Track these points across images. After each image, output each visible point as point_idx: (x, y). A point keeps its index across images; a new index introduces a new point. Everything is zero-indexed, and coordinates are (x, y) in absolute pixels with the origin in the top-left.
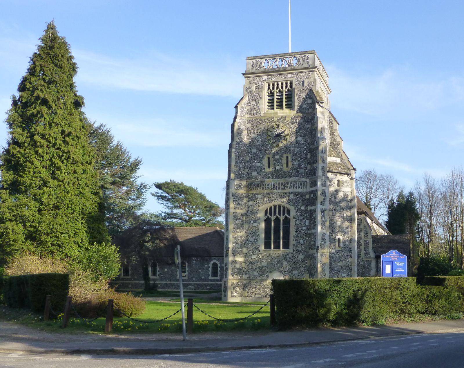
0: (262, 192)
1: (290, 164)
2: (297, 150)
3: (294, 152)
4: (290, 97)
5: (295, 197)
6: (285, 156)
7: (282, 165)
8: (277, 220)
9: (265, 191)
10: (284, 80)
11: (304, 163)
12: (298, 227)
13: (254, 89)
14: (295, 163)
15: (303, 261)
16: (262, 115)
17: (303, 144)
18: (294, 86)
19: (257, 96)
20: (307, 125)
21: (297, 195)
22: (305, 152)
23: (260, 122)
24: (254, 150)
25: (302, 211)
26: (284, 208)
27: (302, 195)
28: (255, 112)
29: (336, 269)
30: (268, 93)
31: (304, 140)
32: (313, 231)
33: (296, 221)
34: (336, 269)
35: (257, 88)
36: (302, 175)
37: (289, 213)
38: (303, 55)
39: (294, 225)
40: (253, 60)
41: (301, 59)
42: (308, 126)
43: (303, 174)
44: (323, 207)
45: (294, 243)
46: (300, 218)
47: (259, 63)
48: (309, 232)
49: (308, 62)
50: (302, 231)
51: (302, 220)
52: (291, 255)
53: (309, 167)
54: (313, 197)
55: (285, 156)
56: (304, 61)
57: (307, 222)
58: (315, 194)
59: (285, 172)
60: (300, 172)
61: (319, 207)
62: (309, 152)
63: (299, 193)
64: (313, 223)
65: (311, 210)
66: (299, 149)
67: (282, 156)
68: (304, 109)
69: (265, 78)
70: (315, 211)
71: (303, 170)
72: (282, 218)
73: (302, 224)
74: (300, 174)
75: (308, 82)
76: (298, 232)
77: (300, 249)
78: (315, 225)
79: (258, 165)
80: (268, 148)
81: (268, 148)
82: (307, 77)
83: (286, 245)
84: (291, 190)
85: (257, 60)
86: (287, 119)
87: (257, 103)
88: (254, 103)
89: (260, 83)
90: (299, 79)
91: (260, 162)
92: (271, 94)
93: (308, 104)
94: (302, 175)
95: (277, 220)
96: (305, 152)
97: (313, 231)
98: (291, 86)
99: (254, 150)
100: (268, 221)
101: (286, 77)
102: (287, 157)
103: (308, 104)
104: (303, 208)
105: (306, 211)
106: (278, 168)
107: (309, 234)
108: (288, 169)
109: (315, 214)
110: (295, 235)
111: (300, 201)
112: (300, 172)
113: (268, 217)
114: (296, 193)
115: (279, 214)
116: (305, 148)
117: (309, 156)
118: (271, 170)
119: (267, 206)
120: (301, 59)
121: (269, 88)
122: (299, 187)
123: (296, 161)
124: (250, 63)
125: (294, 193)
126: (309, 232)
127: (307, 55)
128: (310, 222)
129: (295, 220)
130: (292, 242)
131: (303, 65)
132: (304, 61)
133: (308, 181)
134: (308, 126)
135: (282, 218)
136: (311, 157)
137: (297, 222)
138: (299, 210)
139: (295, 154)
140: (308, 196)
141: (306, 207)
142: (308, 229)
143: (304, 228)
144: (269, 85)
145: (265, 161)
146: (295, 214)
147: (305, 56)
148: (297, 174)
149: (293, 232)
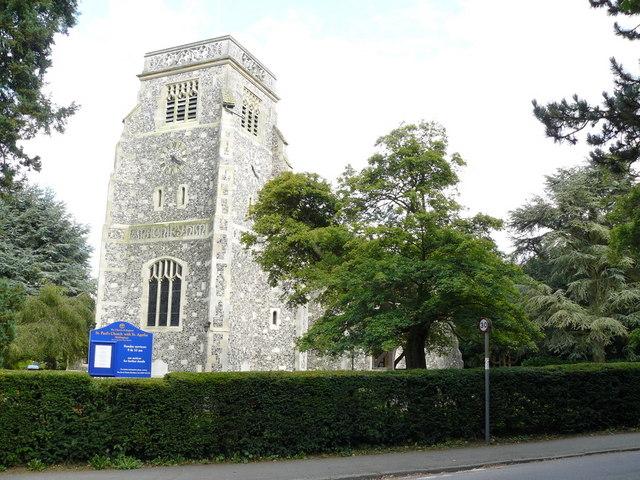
0: (148, 240)
3: (191, 180)
8: (165, 282)
9: (152, 240)
11: (204, 196)
12: (191, 293)
14: (192, 198)
15: (196, 344)
24: (142, 181)
25: (199, 269)
26: (175, 264)
29: (269, 358)
34: (269, 358)
35: (154, 94)
37: (180, 273)
38: (214, 44)
44: (221, 262)
45: (185, 317)
46: (195, 279)
49: (220, 52)
52: (179, 336)
61: (214, 261)
67: (176, 188)
72: (171, 278)
77: (192, 326)
79: (146, 201)
83: (175, 321)
84: (185, 238)
91: (149, 197)
92: (171, 101)
95: (165, 282)
99: (142, 181)
100: (153, 283)
104: (199, 264)
108: (184, 207)
113: (154, 278)
115: (169, 274)
118: (162, 209)
119: (152, 261)
130: (182, 316)
135: (171, 278)
138: (192, 267)
145: (156, 195)
149: (183, 302)
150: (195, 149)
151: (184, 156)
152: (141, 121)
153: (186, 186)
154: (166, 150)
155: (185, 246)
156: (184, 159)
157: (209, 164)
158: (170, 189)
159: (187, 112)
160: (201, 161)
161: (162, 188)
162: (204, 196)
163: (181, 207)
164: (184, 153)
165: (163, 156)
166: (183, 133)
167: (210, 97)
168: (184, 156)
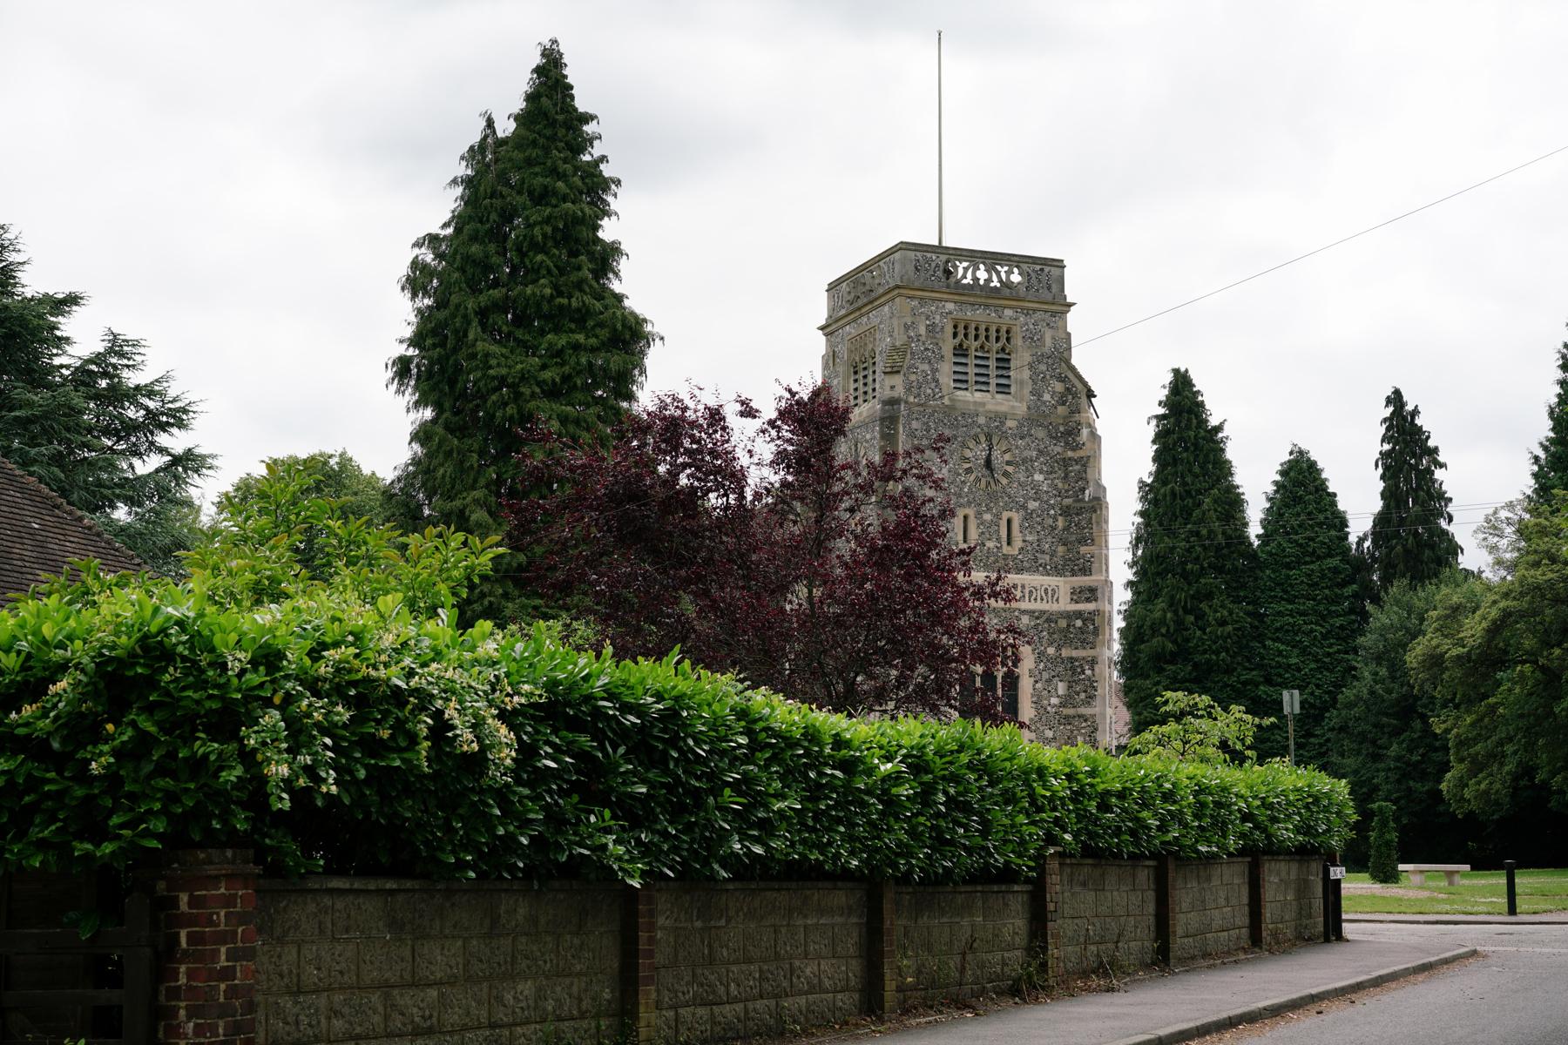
1: (1018, 543)
2: (1033, 505)
3: (1024, 507)
4: (1004, 363)
5: (1033, 623)
6: (1006, 515)
7: (999, 540)
10: (996, 321)
12: (1040, 697)
13: (922, 330)
14: (1029, 538)
16: (946, 401)
17: (1047, 492)
18: (1018, 341)
19: (934, 352)
20: (1055, 445)
21: (1037, 618)
22: (1052, 512)
23: (946, 421)
27: (1050, 618)
28: (929, 391)
30: (955, 349)
31: (1050, 482)
32: (1083, 711)
33: (1036, 682)
35: (931, 329)
36: (1045, 568)
38: (1038, 267)
39: (1032, 691)
40: (918, 254)
41: (1033, 275)
42: (1058, 449)
43: (1048, 567)
46: (1045, 675)
47: (933, 265)
48: (1070, 711)
49: (1049, 288)
50: (1049, 708)
51: (1049, 681)
53: (1061, 549)
54: (1080, 628)
55: (1006, 515)
56: (1040, 282)
57: (1062, 688)
58: (1094, 620)
59: (1006, 557)
60: (1040, 561)
62: (1060, 515)
63: (1043, 612)
64: (1085, 691)
65: (1072, 660)
66: (1037, 504)
67: (998, 516)
68: (1045, 402)
69: (950, 306)
70: (1093, 662)
71: (1048, 557)
73: (1049, 691)
74: (1040, 565)
75: (1053, 338)
76: (1042, 711)
78: (1092, 697)
80: (966, 490)
81: (966, 490)
82: (1048, 325)
84: (1024, 605)
85: (929, 255)
86: (1010, 423)
87: (935, 371)
88: (926, 367)
89: (938, 317)
90: (1031, 326)
93: (1054, 392)
94: (1045, 568)
96: (1052, 512)
97: (1083, 711)
98: (1008, 339)
101: (1000, 313)
102: (1009, 521)
103: (1054, 392)
104: (1051, 651)
105: (1058, 660)
106: (990, 544)
107: (1067, 717)
109: (1093, 670)
110: (1033, 716)
111: (1045, 633)
112: (1040, 561)
114: (1034, 612)
116: (1052, 502)
117: (1061, 523)
120: (1033, 275)
121: (955, 335)
122: (1042, 600)
123: (1030, 533)
124: (911, 261)
125: (1031, 613)
126: (1070, 711)
127: (1047, 269)
128: (1070, 687)
129: (1032, 679)
131: (1038, 290)
132: (1040, 282)
133: (1061, 584)
134: (1058, 449)
136: (1066, 529)
137: (1039, 685)
138: (1041, 656)
139: (1028, 516)
140: (1063, 623)
141: (1059, 648)
142: (1062, 705)
143: (1054, 701)
144: (955, 327)
146: (1032, 666)
147: (1042, 270)
148: (1036, 567)
150: (1027, 453)
151: (1008, 463)
152: (913, 377)
153: (1017, 518)
154: (972, 444)
155: (1025, 620)
156: (1010, 469)
157: (1055, 487)
158: (987, 517)
159: (993, 381)
160: (1038, 477)
161: (970, 512)
162: (1049, 539)
163: (1006, 549)
164: (1007, 457)
165: (968, 454)
166: (1001, 418)
167: (1043, 367)
168: (1008, 463)
